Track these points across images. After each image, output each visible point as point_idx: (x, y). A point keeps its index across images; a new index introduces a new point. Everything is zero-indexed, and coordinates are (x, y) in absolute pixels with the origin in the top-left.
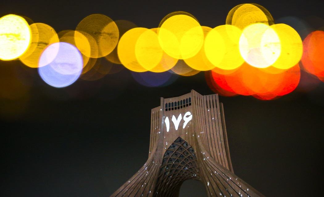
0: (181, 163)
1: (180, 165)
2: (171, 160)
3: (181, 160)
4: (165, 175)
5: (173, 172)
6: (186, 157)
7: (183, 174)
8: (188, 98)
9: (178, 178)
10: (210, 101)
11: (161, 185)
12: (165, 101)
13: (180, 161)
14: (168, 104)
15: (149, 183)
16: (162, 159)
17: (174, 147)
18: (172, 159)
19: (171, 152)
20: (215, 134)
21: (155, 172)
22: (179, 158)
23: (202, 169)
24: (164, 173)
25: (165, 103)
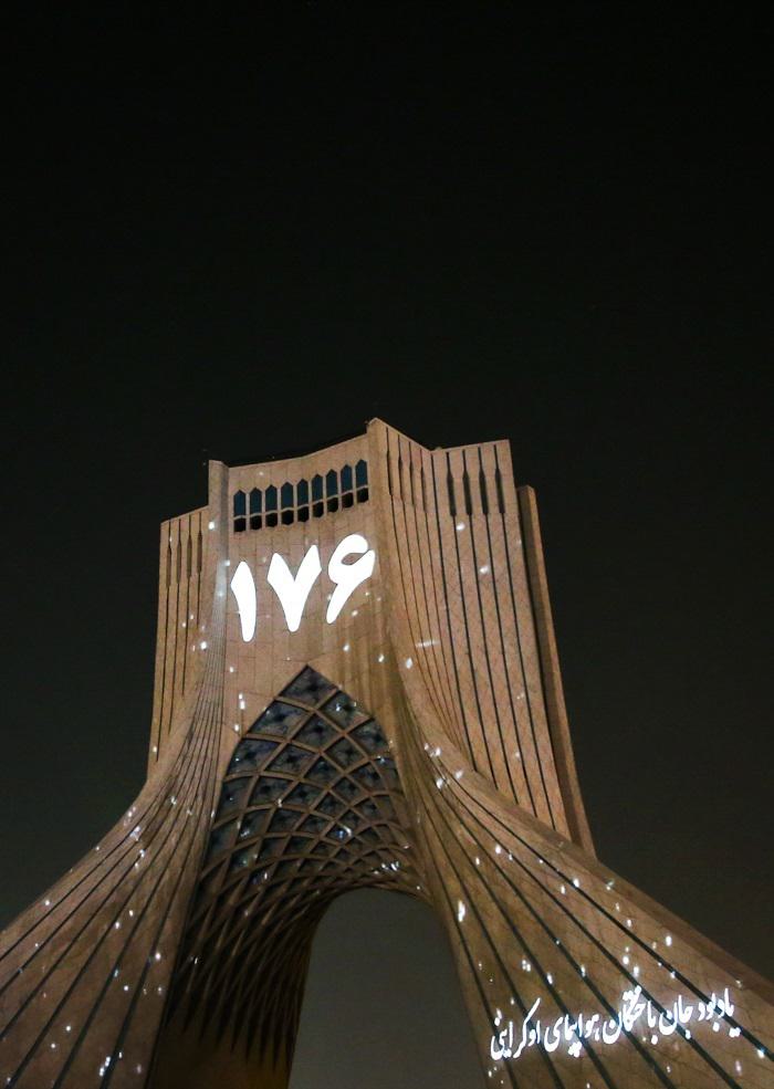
0: (315, 804)
1: (311, 816)
2: (267, 790)
3: (319, 790)
4: (237, 870)
5: (278, 850)
6: (343, 773)
7: (331, 864)
8: (353, 464)
9: (305, 883)
10: (466, 478)
11: (211, 923)
12: (228, 480)
13: (310, 796)
15: (149, 909)
16: (219, 786)
17: (280, 718)
18: (270, 783)
19: (266, 747)
20: (494, 653)
21: (181, 851)
22: (306, 777)
23: (426, 838)
24: (228, 857)
25: (232, 492)
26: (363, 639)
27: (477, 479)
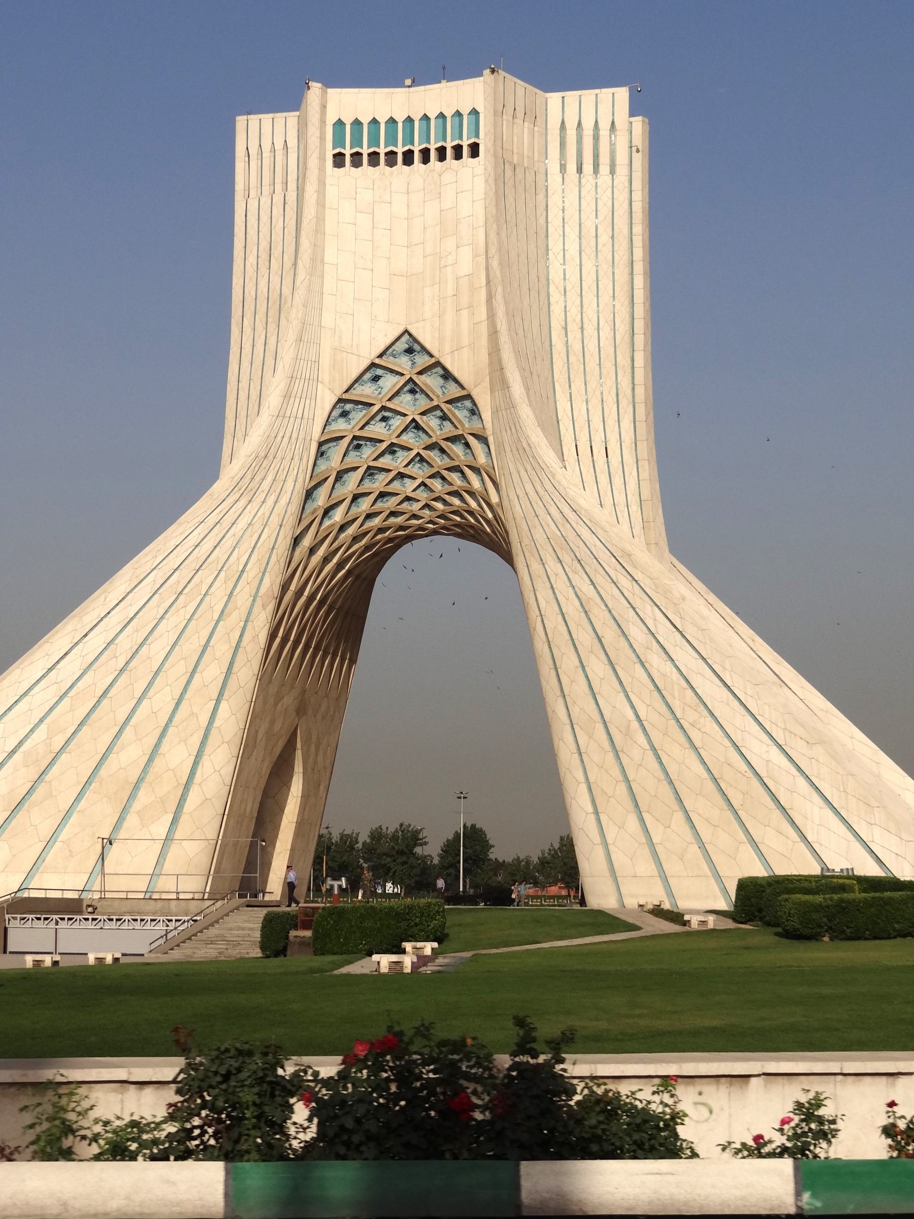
14: (348, 128)
17: (376, 379)
20: (590, 330)
25: (331, 119)
26: (465, 313)
27: (591, 133)
